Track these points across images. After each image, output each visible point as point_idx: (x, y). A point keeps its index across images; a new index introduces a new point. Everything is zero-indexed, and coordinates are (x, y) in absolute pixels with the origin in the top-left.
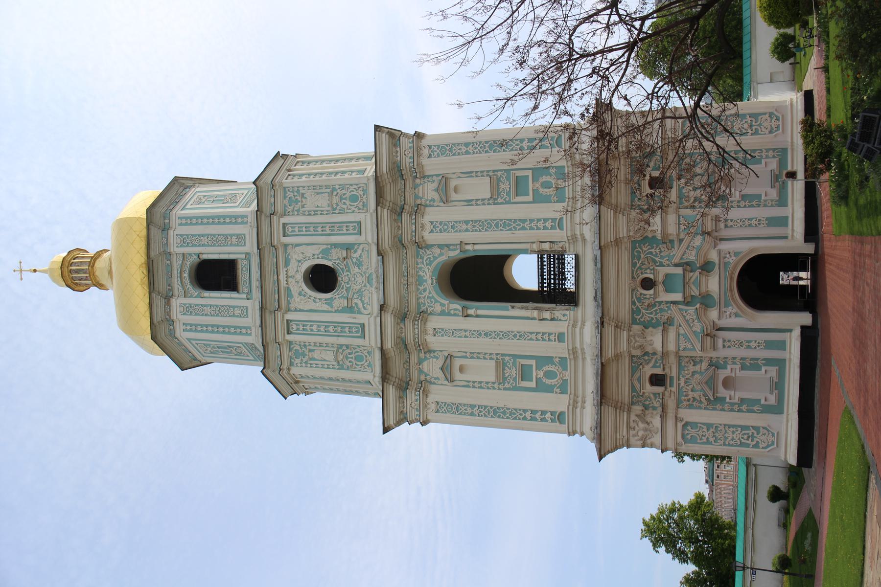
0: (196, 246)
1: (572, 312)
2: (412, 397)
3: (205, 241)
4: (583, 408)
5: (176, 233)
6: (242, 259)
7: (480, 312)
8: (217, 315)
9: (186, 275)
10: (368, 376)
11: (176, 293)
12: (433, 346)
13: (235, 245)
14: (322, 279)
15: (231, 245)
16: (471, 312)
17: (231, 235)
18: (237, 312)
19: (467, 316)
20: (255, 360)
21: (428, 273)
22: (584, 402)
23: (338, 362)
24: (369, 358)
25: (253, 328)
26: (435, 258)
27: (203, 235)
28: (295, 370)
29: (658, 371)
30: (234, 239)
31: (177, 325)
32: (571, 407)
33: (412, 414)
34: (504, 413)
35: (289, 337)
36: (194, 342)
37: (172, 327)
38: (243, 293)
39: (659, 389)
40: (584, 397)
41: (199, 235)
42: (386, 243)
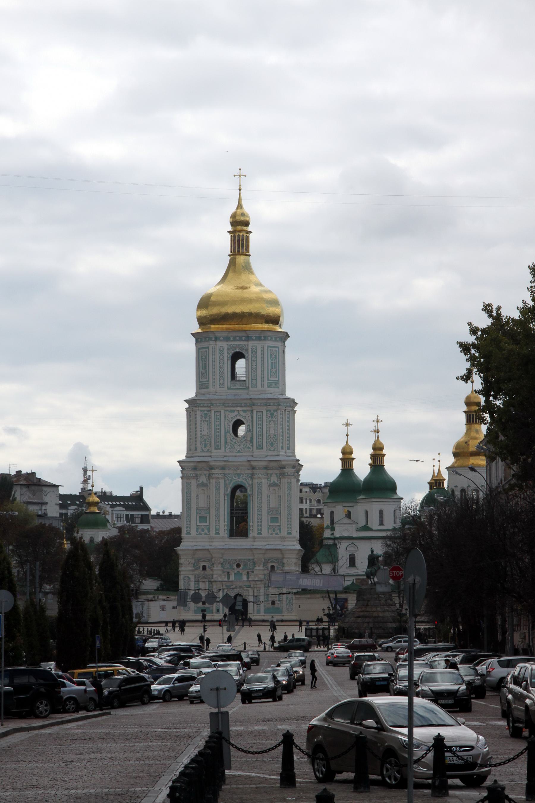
2: (191, 472)
3: (254, 363)
9: (238, 350)
10: (199, 449)
12: (211, 480)
15: (252, 380)
16: (226, 497)
17: (256, 380)
18: (222, 382)
20: (200, 382)
21: (241, 480)
24: (205, 450)
25: (214, 390)
27: (256, 363)
28: (198, 412)
29: (207, 569)
30: (254, 381)
33: (184, 472)
35: (213, 412)
36: (207, 350)
37: (213, 339)
39: (201, 569)
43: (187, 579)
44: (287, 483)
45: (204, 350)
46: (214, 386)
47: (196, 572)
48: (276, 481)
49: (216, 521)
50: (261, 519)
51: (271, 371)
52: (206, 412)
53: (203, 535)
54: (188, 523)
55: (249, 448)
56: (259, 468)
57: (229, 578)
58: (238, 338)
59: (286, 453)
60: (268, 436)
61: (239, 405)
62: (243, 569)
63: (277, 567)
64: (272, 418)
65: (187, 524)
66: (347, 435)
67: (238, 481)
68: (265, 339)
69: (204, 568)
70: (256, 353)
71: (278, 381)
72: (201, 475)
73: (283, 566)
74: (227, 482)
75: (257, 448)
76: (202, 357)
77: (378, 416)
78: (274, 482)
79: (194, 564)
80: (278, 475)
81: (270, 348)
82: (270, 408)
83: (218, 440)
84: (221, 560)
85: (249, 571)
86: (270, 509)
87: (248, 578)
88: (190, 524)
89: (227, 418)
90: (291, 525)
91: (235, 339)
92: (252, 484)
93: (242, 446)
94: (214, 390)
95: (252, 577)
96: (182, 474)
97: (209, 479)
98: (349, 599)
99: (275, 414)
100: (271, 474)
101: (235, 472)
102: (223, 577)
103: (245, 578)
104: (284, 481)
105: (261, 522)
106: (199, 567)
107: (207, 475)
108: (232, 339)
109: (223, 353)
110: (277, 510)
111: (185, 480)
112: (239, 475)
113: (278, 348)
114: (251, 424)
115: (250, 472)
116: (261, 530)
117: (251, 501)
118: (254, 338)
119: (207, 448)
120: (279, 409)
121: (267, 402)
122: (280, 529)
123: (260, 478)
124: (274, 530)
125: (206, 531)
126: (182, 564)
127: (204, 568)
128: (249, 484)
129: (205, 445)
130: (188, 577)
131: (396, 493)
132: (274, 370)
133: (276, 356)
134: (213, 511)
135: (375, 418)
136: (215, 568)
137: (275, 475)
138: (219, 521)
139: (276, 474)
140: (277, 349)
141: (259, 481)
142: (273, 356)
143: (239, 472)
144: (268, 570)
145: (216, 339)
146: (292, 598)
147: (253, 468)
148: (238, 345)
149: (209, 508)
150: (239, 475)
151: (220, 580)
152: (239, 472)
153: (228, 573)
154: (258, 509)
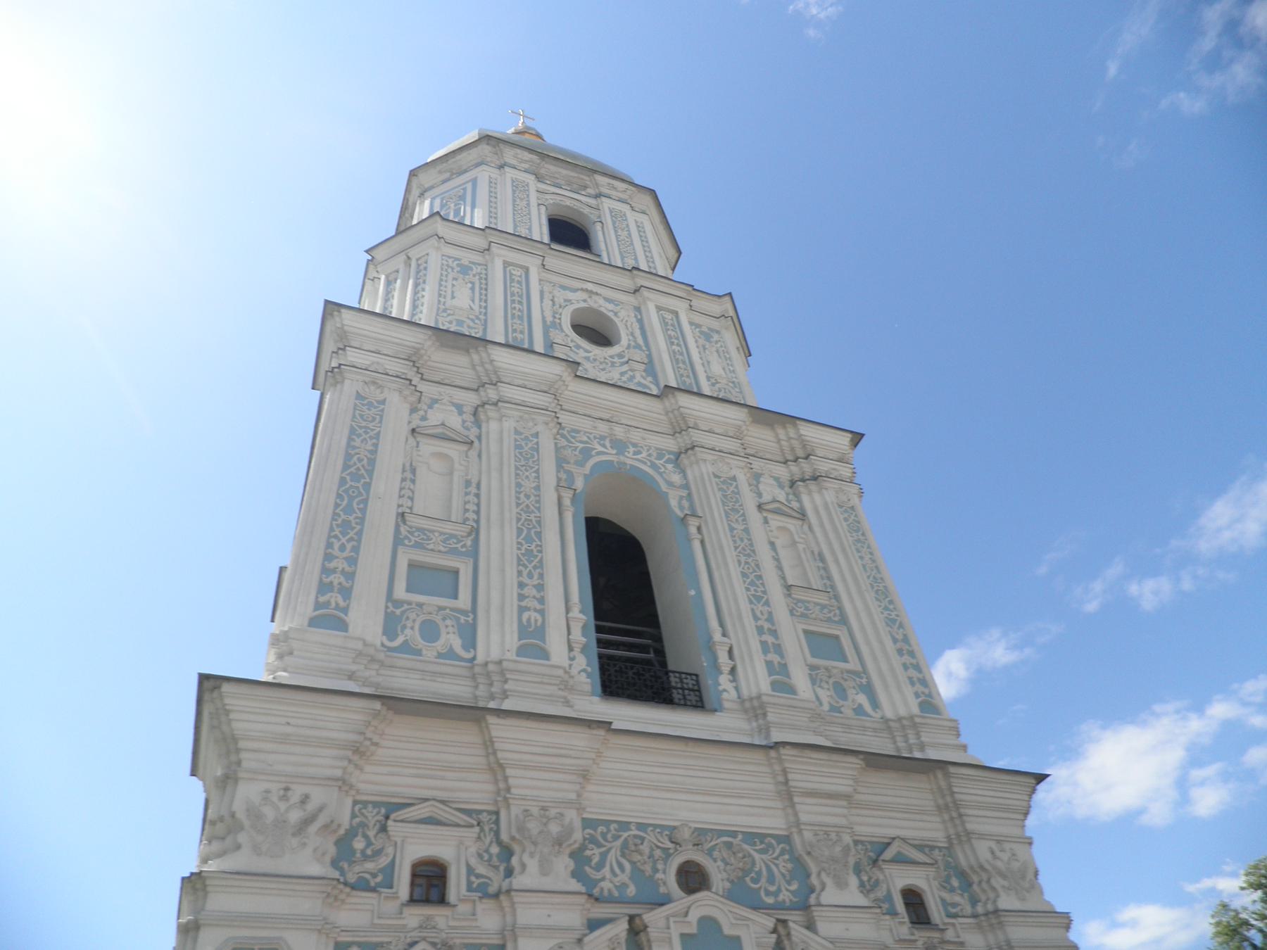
1: (588, 688)
11: (542, 186)
26: (661, 474)
32: (359, 646)
49: (521, 585)
53: (429, 654)
54: (339, 564)
63: (943, 900)
78: (774, 501)
80: (787, 484)
84: (572, 816)
88: (350, 576)
89: (547, 295)
99: (716, 337)
105: (774, 633)
107: (468, 409)
110: (823, 607)
114: (638, 333)
122: (869, 690)
124: (841, 691)
125: (451, 639)
127: (430, 882)
134: (499, 542)
138: (540, 587)
139: (777, 479)
143: (619, 432)
144: (893, 913)
147: (680, 426)
149: (475, 532)
154: (744, 575)
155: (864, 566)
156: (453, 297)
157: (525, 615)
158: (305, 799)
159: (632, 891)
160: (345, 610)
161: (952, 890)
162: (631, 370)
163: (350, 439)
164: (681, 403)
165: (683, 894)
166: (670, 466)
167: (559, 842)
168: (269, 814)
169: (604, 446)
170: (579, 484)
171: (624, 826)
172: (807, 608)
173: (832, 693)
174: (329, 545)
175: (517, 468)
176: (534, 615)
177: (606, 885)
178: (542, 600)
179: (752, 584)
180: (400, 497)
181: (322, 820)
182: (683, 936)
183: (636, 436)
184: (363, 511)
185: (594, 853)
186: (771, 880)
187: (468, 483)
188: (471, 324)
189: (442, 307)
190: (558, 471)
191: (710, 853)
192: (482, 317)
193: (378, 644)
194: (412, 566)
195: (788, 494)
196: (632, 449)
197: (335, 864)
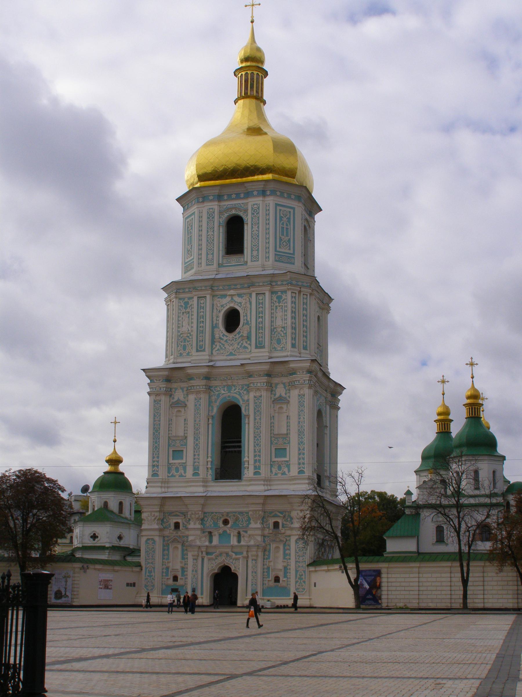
0: (252, 220)
1: (211, 479)
2: (163, 385)
3: (255, 228)
4: (161, 487)
5: (261, 202)
6: (244, 258)
7: (210, 426)
8: (208, 241)
9: (234, 212)
13: (252, 253)
14: (232, 320)
15: (252, 251)
16: (210, 421)
17: (258, 250)
18: (210, 257)
19: (208, 419)
20: (185, 263)
22: (165, 487)
23: (182, 334)
25: (200, 269)
26: (241, 397)
27: (258, 227)
30: (255, 253)
31: (201, 205)
32: (161, 480)
34: (156, 443)
36: (193, 217)
37: (201, 200)
38: (223, 259)
39: (172, 527)
40: (168, 487)
41: (258, 223)
42: (248, 368)
43: (151, 543)
44: (299, 395)
45: (190, 218)
46: (200, 264)
47: (166, 533)
48: (283, 395)
49: (195, 455)
50: (260, 452)
51: (281, 239)
52: (186, 300)
55: (245, 347)
56: (260, 376)
57: (211, 541)
58: (234, 196)
59: (300, 354)
60: (273, 330)
61: (233, 287)
62: (231, 527)
63: (283, 524)
64: (279, 302)
65: (154, 461)
66: (443, 394)
67: (229, 396)
68: (273, 193)
69: (177, 526)
70: (258, 213)
71: (293, 254)
72: (176, 389)
73: (292, 523)
74: (213, 398)
75: (257, 347)
76: (188, 228)
77: (472, 358)
78: (280, 396)
79: (162, 520)
80: (288, 384)
81: (279, 208)
82: (277, 288)
83: (201, 338)
85: (239, 530)
86: (274, 437)
87: (239, 541)
88: (158, 461)
89: (215, 307)
90: (303, 459)
91: (230, 198)
92: (248, 400)
93: (236, 346)
94: (200, 269)
95: (246, 539)
96: (150, 388)
97: (187, 395)
98: (384, 571)
99: (284, 297)
100: (277, 384)
101: (225, 384)
102: (204, 539)
103: (234, 541)
104: (294, 393)
105: (260, 456)
106: (170, 525)
107: (185, 389)
108: (226, 197)
109: (213, 218)
111: (153, 397)
112: (229, 387)
113: (294, 209)
115: (246, 382)
116: (259, 468)
117: (247, 425)
118: (255, 193)
119: (187, 351)
120: (288, 289)
121: (272, 280)
122: (288, 466)
123: (258, 389)
124: (279, 468)
125: (182, 471)
126: (144, 520)
127: (177, 526)
128: (243, 400)
129: (184, 348)
130: (152, 539)
131: (496, 451)
132: (287, 238)
133: (289, 219)
135: (469, 361)
136: (191, 526)
137: (282, 386)
138: (199, 455)
139: (284, 384)
140: (292, 211)
141: (258, 394)
142: (285, 219)
143: (229, 383)
145: (205, 199)
146: (304, 571)
147: (250, 375)
148: (232, 205)
150: (229, 387)
151: (198, 543)
152: (229, 383)
153: (210, 533)
154: (255, 437)
155: (299, 422)
156: (182, 326)
157: (195, 464)
158: (154, 515)
159: (213, 525)
160: (158, 471)
161: (287, 521)
162: (242, 340)
163: (154, 418)
164: (247, 368)
165: (223, 526)
166: (245, 392)
167: (197, 519)
168: (149, 518)
169: (224, 390)
170: (215, 410)
171: (212, 513)
172: (278, 441)
173: (277, 469)
174: (153, 454)
175: (195, 415)
176: (197, 464)
177: (208, 525)
178: (199, 459)
179: (258, 440)
180: (169, 431)
181: (157, 518)
182: (220, 535)
183: (234, 384)
184: (159, 442)
185: (206, 519)
186: (242, 522)
187: (185, 419)
188: (189, 340)
189: (179, 334)
190: (209, 407)
191: (230, 517)
192: (192, 333)
193: (166, 476)
194: (173, 451)
195: (286, 390)
196: (233, 388)
197: (161, 524)
